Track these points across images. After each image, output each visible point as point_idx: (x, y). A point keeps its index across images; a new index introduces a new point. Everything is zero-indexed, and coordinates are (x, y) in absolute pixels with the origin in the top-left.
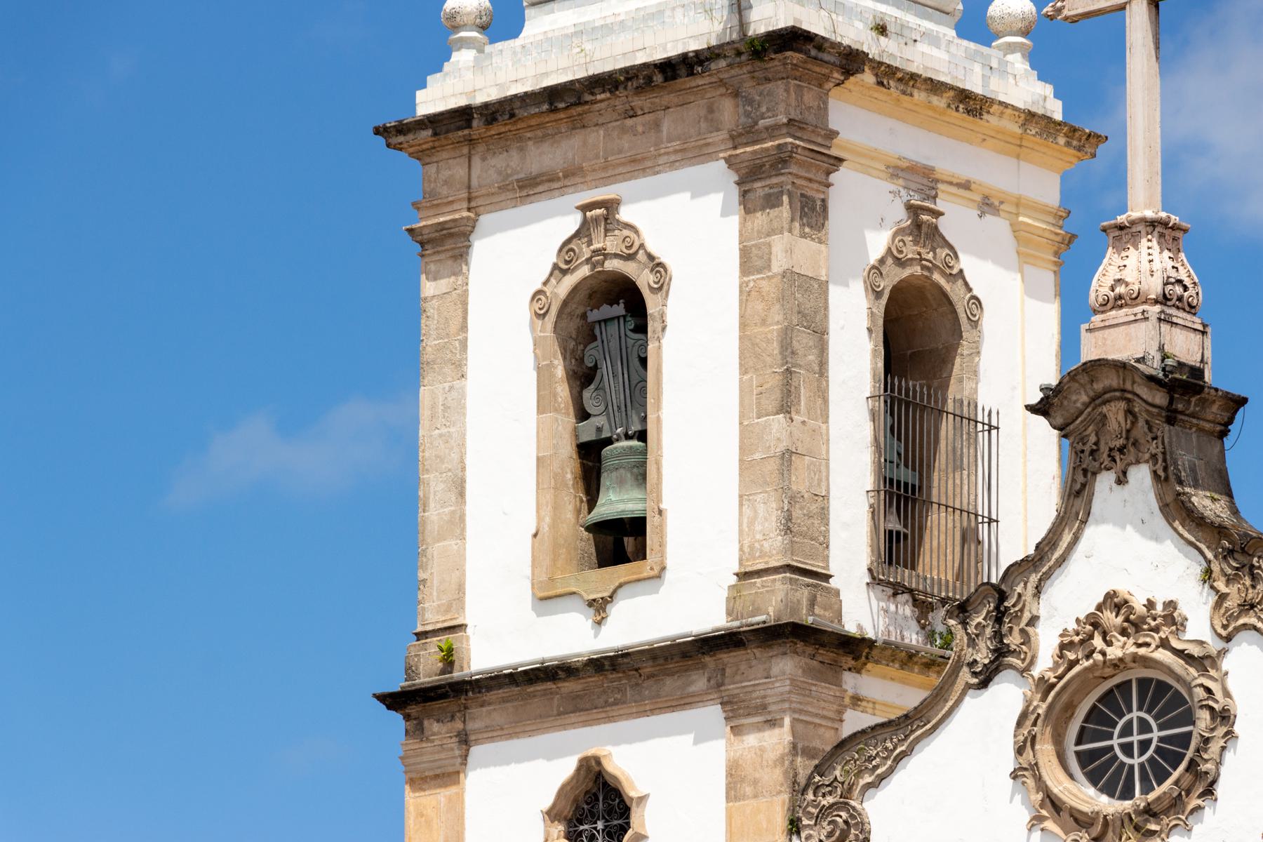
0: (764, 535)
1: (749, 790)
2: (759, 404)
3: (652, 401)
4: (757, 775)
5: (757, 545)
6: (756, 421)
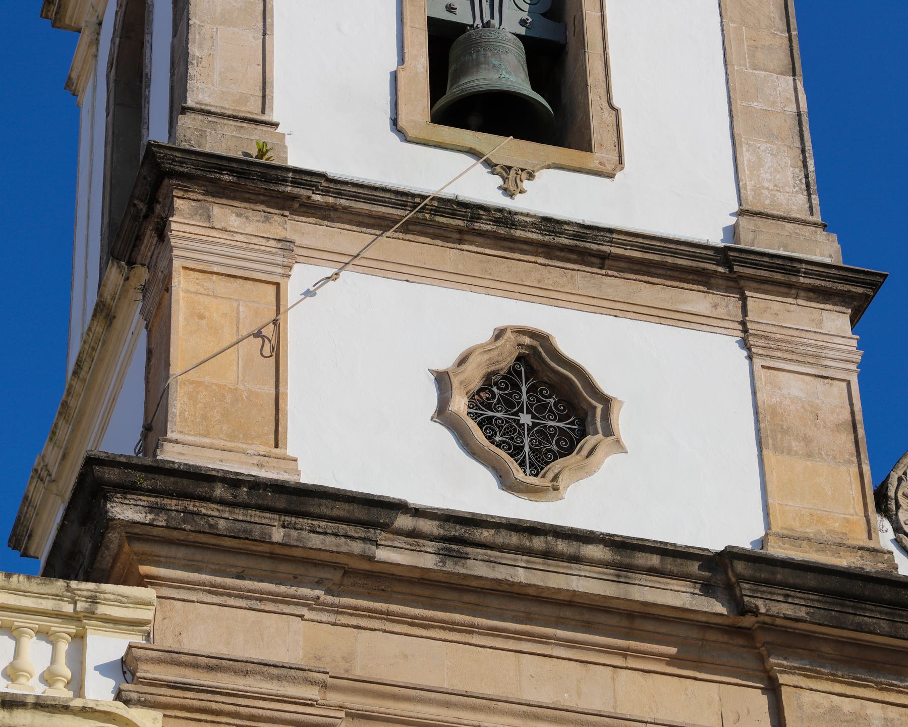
0: (776, 186)
5: (765, 191)
6: (751, 71)
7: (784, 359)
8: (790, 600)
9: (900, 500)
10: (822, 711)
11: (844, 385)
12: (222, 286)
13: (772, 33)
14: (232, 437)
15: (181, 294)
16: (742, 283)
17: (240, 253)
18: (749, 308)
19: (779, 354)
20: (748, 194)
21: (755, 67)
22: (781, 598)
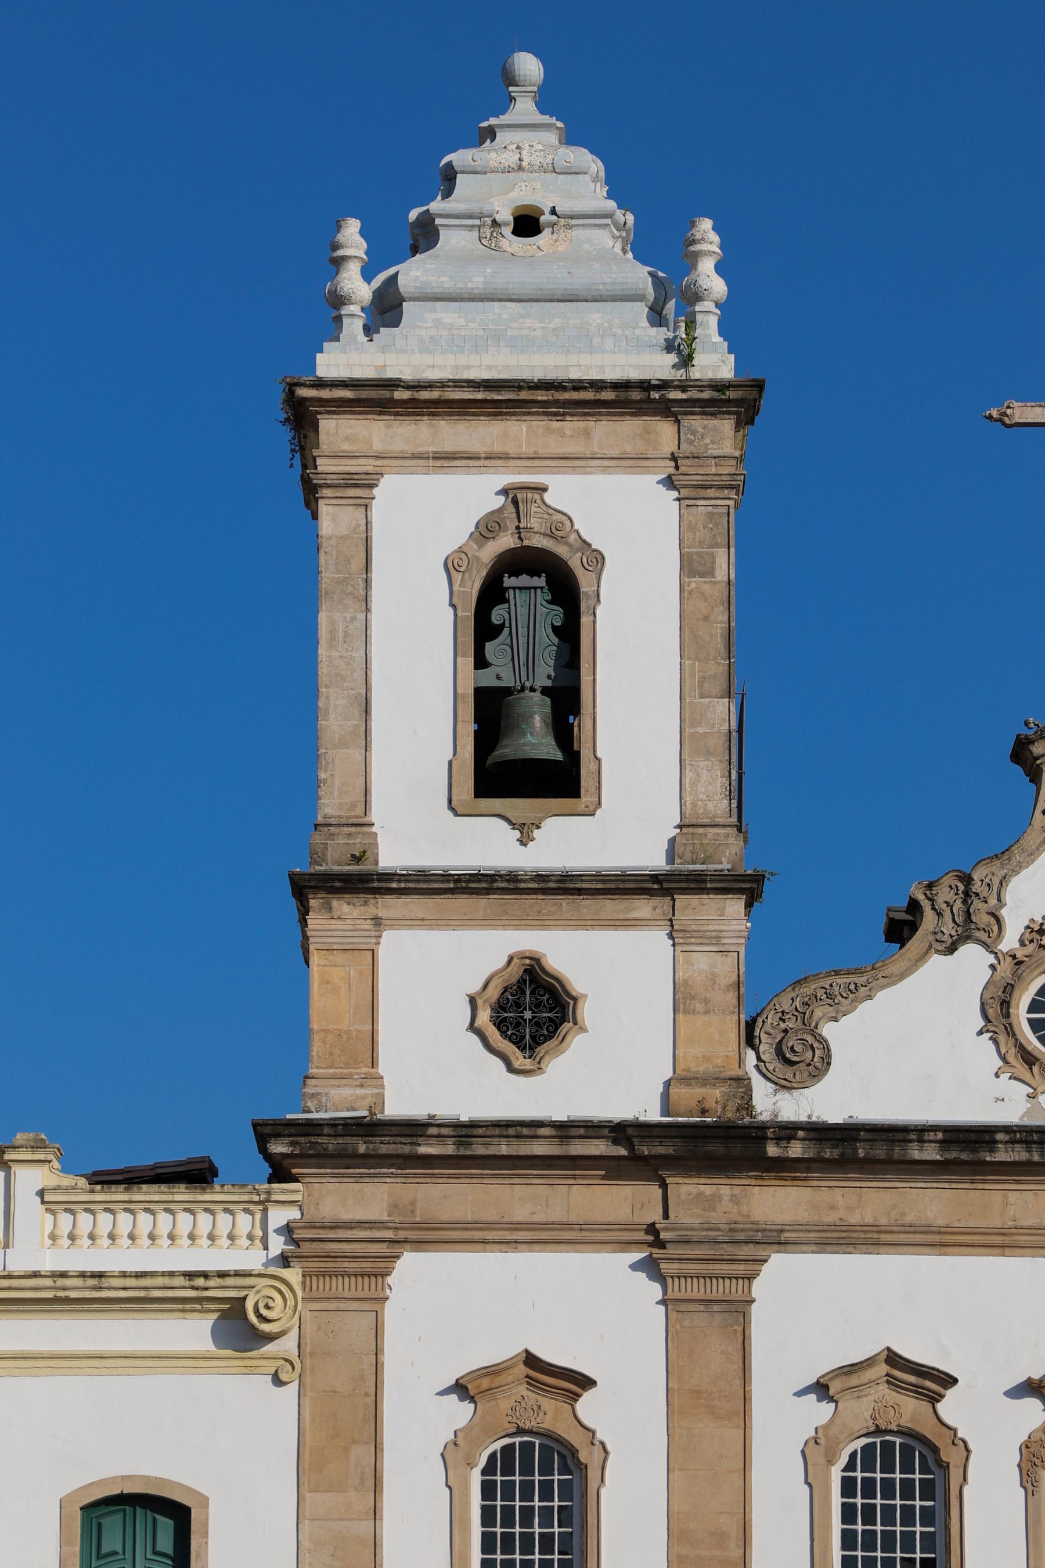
0: (708, 796)
1: (699, 1007)
2: (701, 686)
3: (586, 665)
4: (708, 996)
5: (700, 803)
6: (699, 700)
7: (697, 944)
8: (663, 1144)
9: (761, 1037)
10: (691, 1196)
11: (736, 954)
12: (339, 958)
13: (718, 662)
14: (347, 1066)
15: (315, 968)
16: (671, 891)
17: (349, 934)
18: (676, 907)
19: (693, 940)
20: (688, 811)
21: (702, 696)
22: (657, 1144)
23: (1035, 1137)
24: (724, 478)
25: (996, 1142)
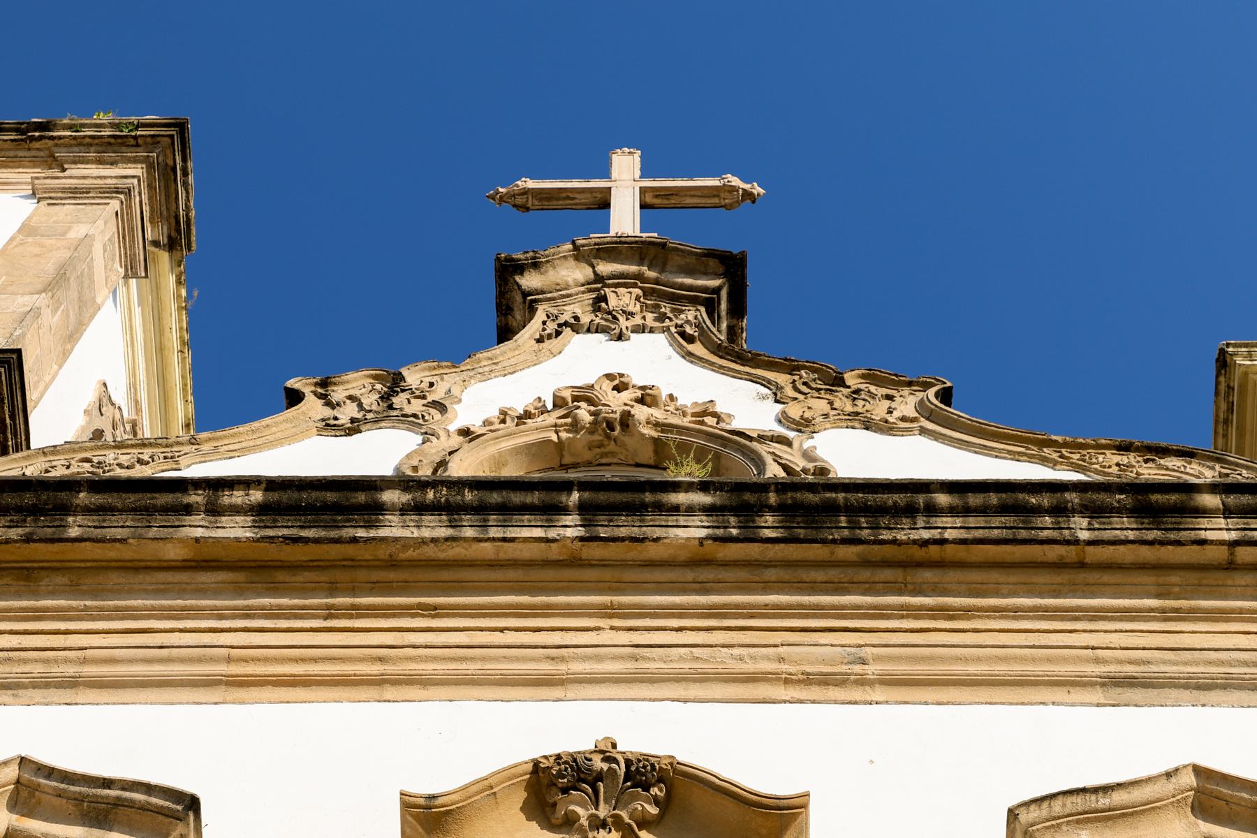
23: (469, 496)
24: (109, 181)
25: (379, 509)
